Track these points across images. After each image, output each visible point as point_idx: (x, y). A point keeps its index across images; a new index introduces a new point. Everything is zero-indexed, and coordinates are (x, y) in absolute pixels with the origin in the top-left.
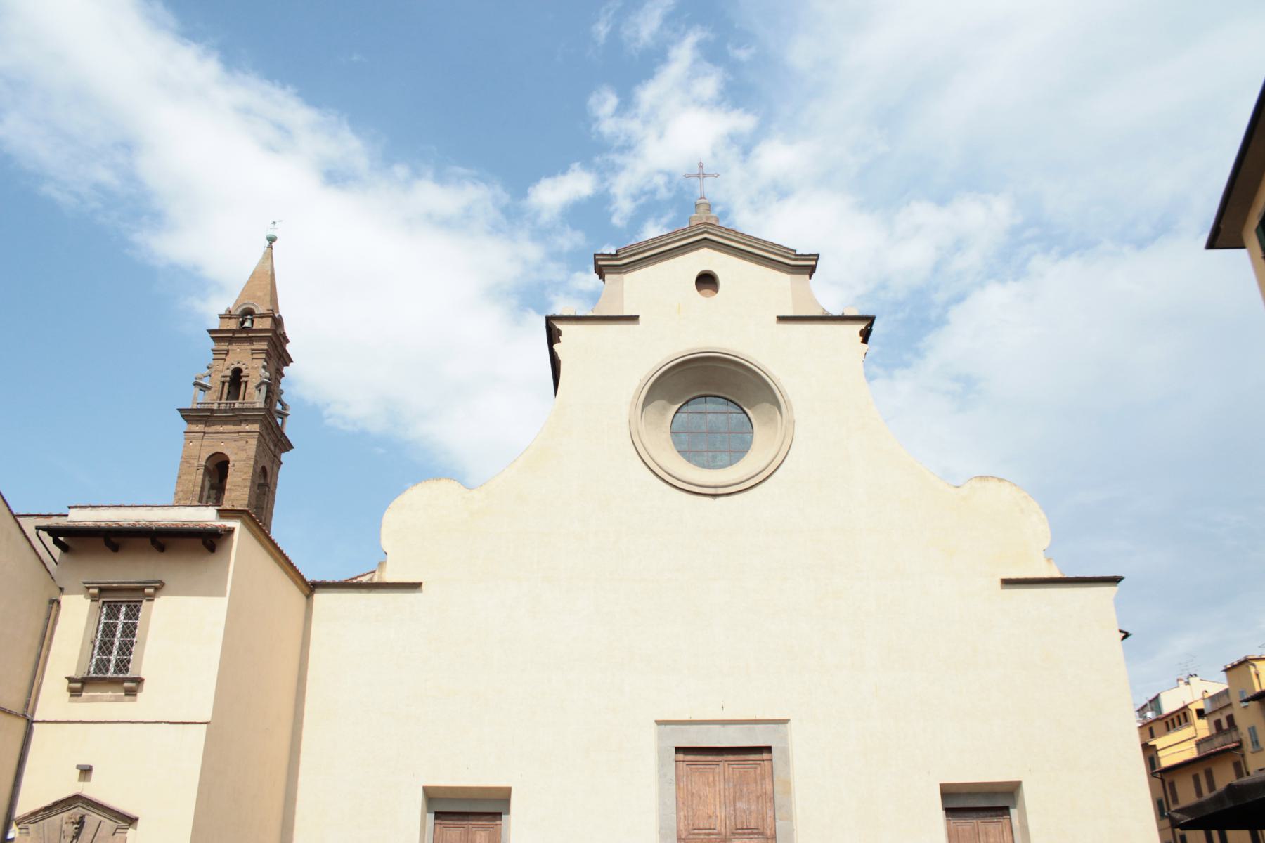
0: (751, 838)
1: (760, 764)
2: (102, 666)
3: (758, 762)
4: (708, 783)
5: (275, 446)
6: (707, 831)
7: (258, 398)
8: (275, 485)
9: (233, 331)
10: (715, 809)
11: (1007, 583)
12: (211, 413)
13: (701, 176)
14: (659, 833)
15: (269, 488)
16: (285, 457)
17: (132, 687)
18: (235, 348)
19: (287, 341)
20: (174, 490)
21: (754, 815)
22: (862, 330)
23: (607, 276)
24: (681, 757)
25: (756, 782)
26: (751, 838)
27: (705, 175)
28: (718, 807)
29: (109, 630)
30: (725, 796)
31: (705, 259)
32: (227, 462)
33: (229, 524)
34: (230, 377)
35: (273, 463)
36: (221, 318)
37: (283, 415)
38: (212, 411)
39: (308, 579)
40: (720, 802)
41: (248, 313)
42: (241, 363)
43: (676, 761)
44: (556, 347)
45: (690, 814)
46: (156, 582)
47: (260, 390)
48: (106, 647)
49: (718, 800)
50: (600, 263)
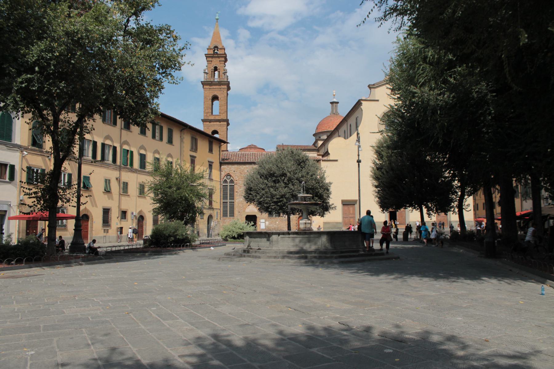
18: (214, 60)
20: (203, 107)
38: (212, 82)
41: (216, 47)
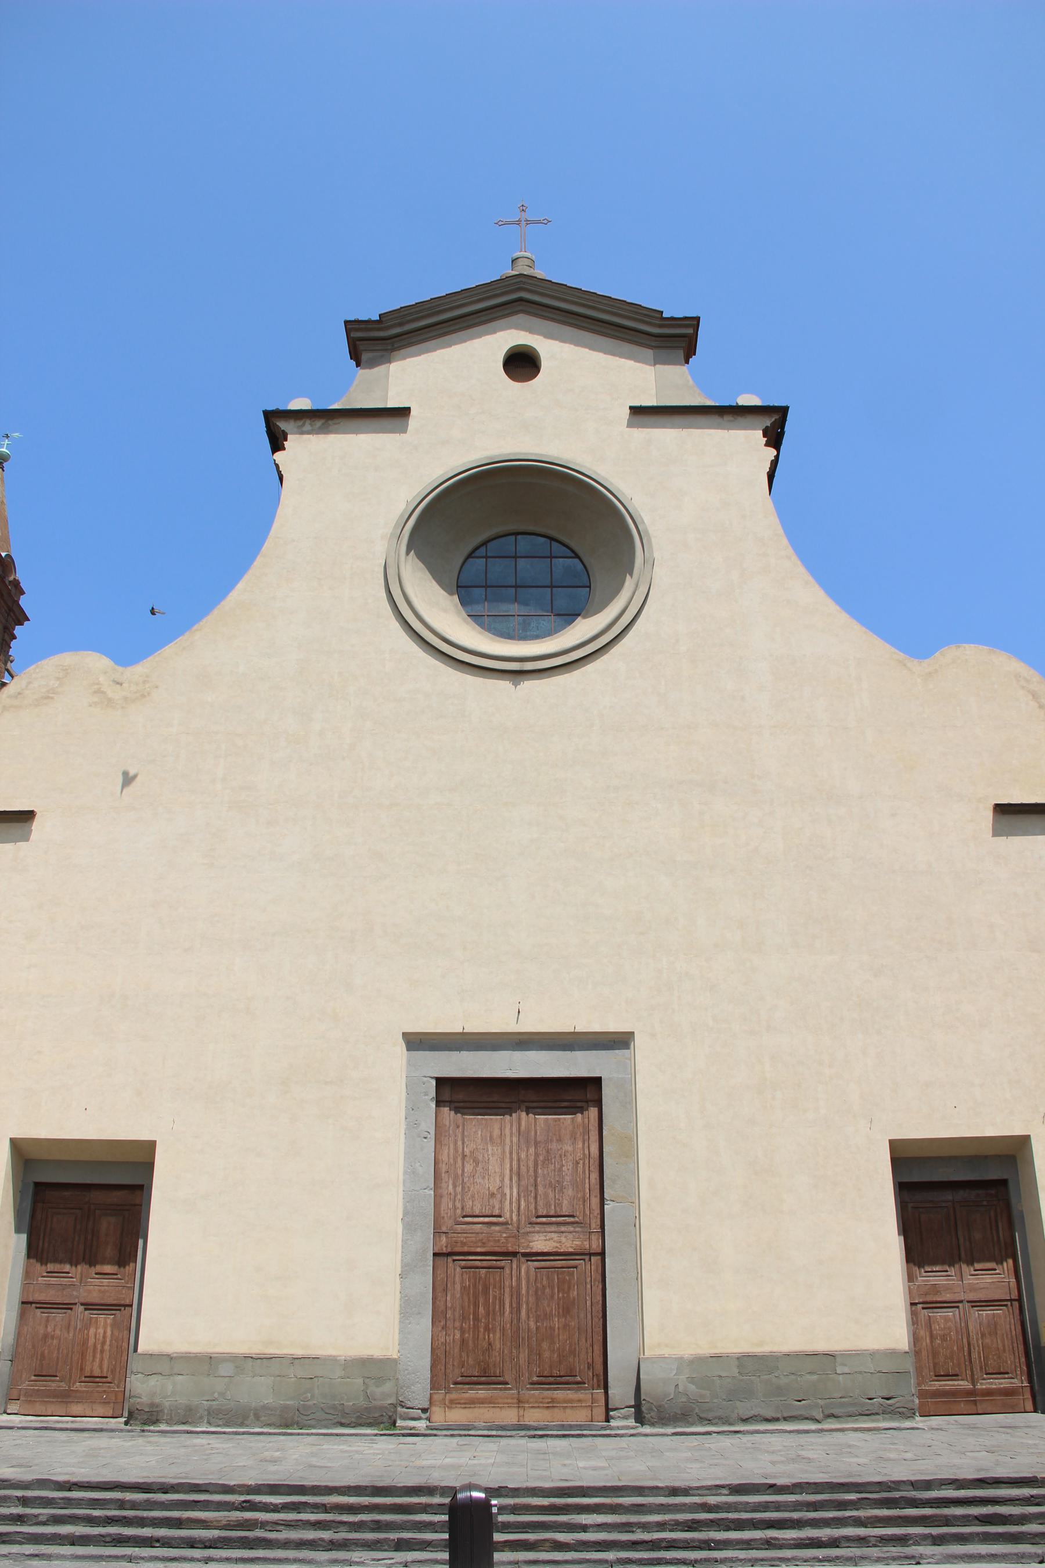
0: (562, 1232)
3: (579, 1104)
4: (491, 1137)
6: (487, 1220)
10: (502, 1181)
13: (523, 223)
19: (22, 593)
21: (569, 1192)
22: (767, 427)
25: (573, 1136)
26: (562, 1232)
27: (528, 222)
30: (519, 1160)
40: (511, 1170)
45: (459, 1189)
50: (355, 334)
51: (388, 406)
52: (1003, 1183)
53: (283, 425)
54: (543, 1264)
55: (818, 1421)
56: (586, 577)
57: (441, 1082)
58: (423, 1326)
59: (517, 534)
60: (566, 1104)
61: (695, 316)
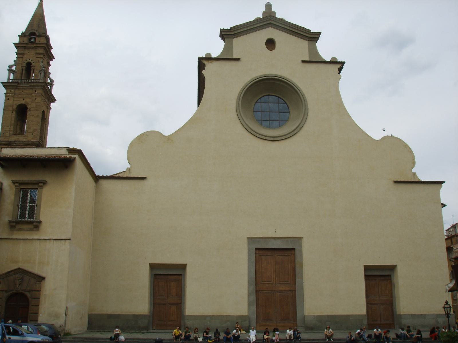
1: (290, 255)
2: (23, 216)
3: (290, 255)
5: (48, 101)
6: (268, 283)
7: (40, 78)
8: (49, 119)
9: (26, 44)
11: (396, 182)
12: (18, 84)
14: (248, 283)
15: (46, 120)
16: (52, 105)
17: (36, 225)
19: (52, 48)
22: (339, 68)
23: (225, 39)
24: (257, 252)
28: (272, 273)
29: (24, 201)
31: (269, 33)
32: (27, 108)
33: (73, 156)
34: (26, 67)
35: (47, 108)
36: (19, 37)
37: (51, 84)
38: (18, 83)
39: (97, 175)
42: (31, 60)
43: (255, 254)
44: (203, 72)
46: (43, 181)
47: (41, 74)
48: (23, 208)
49: (272, 270)
51: (234, 58)
52: (390, 276)
53: (205, 62)
54: (281, 293)
55: (345, 330)
56: (288, 110)
57: (256, 249)
58: (254, 308)
59: (269, 95)
60: (286, 255)
61: (320, 32)
